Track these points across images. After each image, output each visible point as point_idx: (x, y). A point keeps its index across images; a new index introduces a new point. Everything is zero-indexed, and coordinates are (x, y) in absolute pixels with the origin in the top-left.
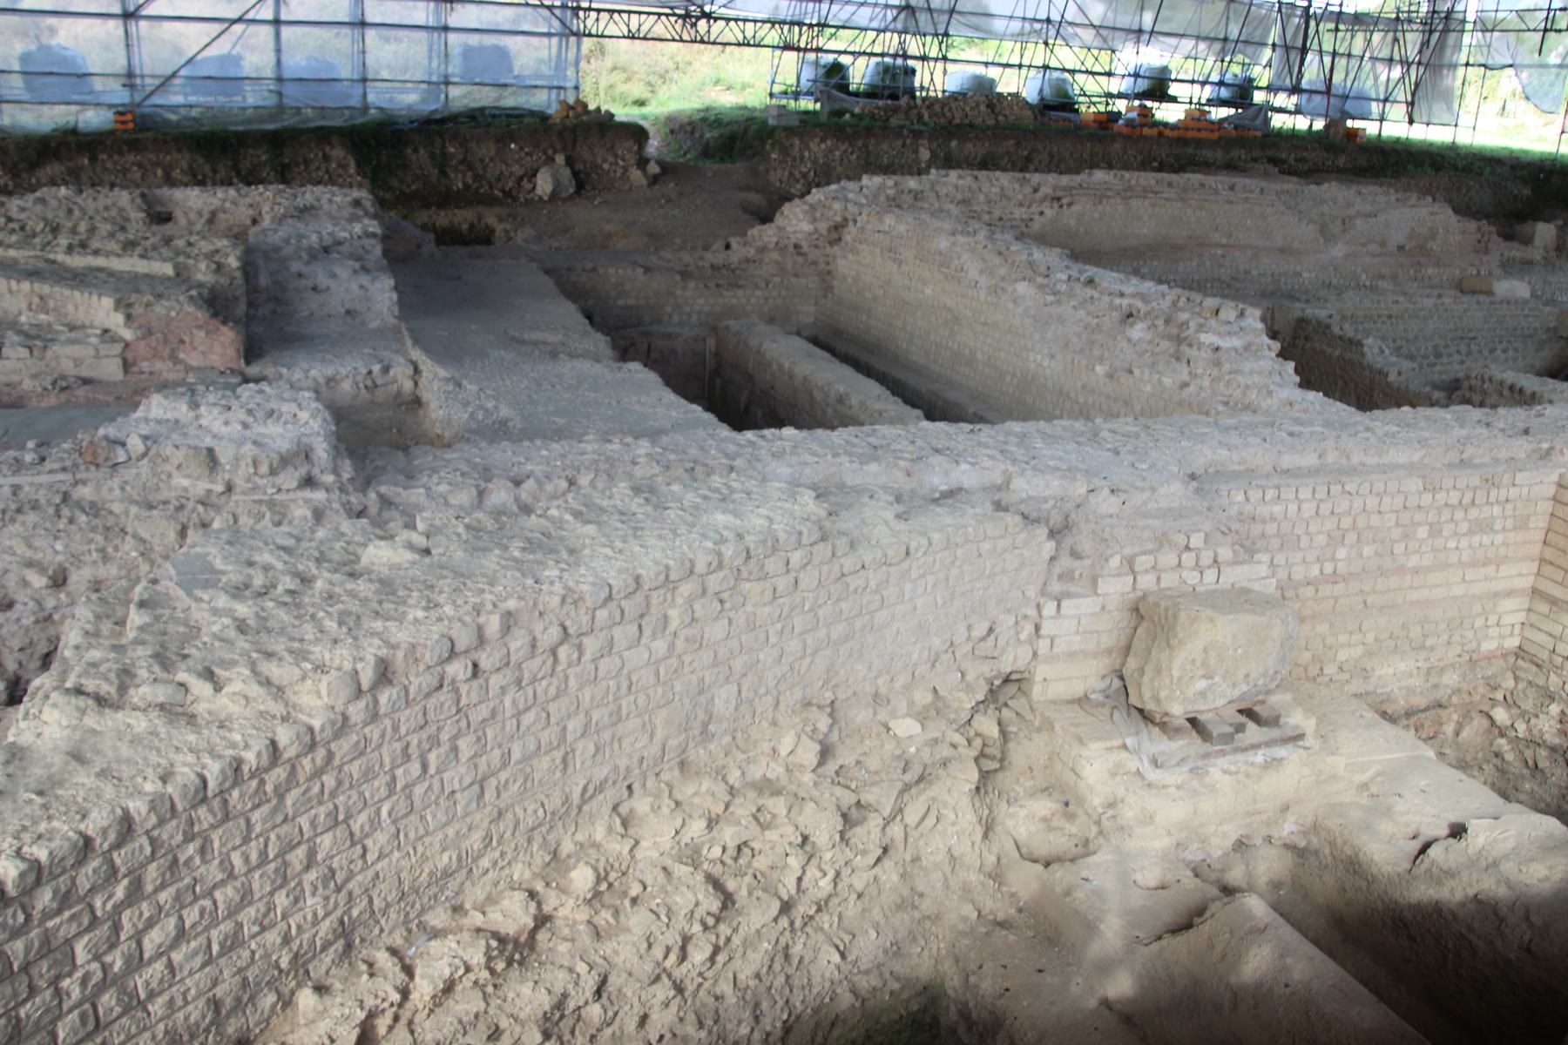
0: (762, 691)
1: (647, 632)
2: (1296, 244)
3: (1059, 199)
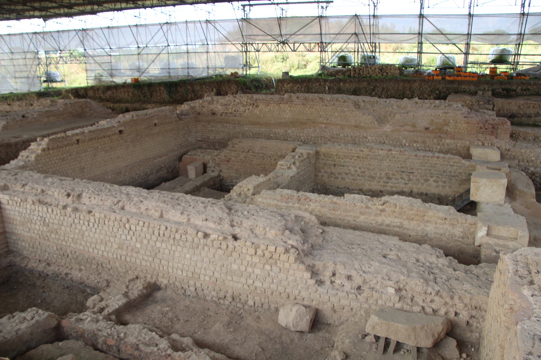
2: (362, 124)
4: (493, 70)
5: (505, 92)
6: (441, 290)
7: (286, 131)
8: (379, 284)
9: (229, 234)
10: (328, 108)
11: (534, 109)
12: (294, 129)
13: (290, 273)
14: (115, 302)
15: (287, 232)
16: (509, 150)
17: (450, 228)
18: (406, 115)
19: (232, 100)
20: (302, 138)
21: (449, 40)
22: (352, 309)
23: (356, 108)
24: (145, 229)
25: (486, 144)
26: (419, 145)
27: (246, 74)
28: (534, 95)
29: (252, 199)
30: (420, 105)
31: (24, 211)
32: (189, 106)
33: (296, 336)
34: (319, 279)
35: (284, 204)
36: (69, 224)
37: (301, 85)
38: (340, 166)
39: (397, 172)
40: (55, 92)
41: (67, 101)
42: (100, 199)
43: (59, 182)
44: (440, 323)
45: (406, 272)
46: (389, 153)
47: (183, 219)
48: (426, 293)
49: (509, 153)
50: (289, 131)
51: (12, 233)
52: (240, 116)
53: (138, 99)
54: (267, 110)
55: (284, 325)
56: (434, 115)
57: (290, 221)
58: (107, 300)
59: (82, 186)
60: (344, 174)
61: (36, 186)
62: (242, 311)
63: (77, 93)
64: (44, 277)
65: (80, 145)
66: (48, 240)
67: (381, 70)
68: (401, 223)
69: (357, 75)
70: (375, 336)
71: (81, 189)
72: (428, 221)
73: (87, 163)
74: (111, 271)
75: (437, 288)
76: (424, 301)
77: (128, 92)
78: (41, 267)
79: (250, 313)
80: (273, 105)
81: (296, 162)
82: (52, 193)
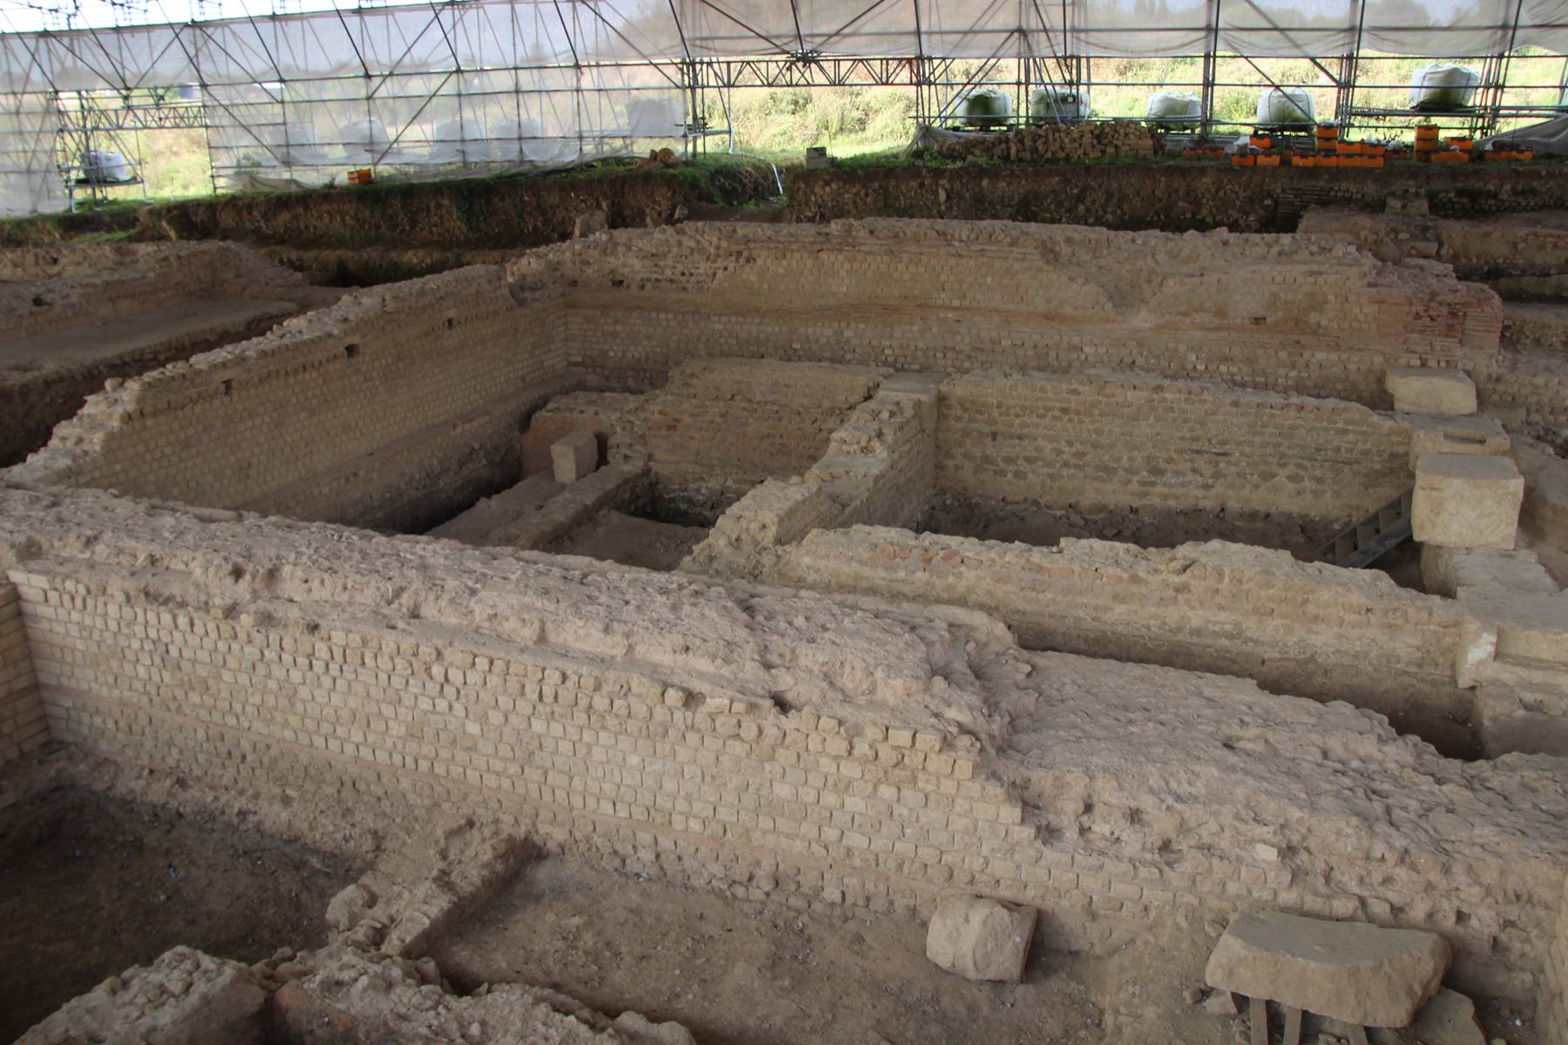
2: (1067, 310)
4: (1428, 133)
5: (1465, 200)
6: (1412, 848)
7: (839, 333)
8: (1227, 834)
9: (760, 692)
10: (964, 261)
11: (1558, 252)
12: (862, 326)
13: (958, 809)
14: (417, 908)
15: (939, 682)
16: (1498, 380)
17: (1381, 637)
18: (1197, 280)
19: (673, 242)
20: (887, 351)
21: (1297, 46)
22: (1146, 909)
23: (1047, 262)
24: (494, 680)
25: (1433, 363)
26: (1235, 370)
27: (695, 154)
28: (1549, 207)
29: (779, 557)
30: (1237, 251)
31: (99, 623)
32: (543, 262)
33: (982, 996)
34: (1044, 822)
35: (882, 573)
36: (246, 664)
37: (864, 186)
38: (1012, 437)
39: (1180, 452)
40: (114, 215)
41: (166, 249)
42: (340, 584)
43: (198, 528)
44: (1426, 953)
45: (1303, 796)
46: (1155, 396)
47: (613, 646)
48: (1368, 858)
49: (1501, 387)
50: (848, 333)
51: (59, 689)
52: (700, 289)
53: (373, 234)
54: (781, 271)
55: (945, 963)
56: (1279, 279)
57: (938, 645)
58: (388, 903)
59: (276, 541)
60: (1021, 462)
61: (130, 543)
62: (805, 918)
63: (190, 218)
64: (169, 822)
65: (235, 398)
66: (179, 709)
67: (1098, 137)
68: (1237, 625)
69: (1027, 155)
70: (1233, 994)
71: (272, 552)
72: (1316, 618)
73: (256, 450)
74: (385, 804)
75: (1400, 842)
76: (1361, 880)
77: (343, 214)
78: (158, 792)
79: (831, 925)
80: (797, 256)
81: (885, 431)
82: (182, 567)
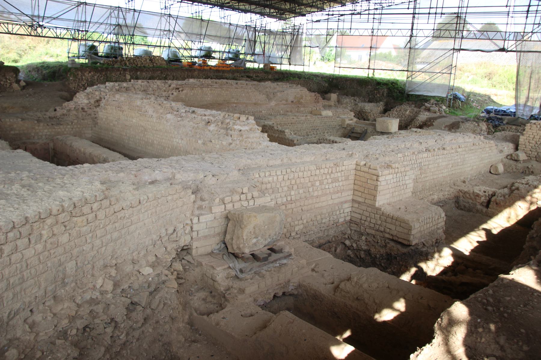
0: (86, 263)
1: (33, 241)
3: (178, 89)
80: (197, 89)
